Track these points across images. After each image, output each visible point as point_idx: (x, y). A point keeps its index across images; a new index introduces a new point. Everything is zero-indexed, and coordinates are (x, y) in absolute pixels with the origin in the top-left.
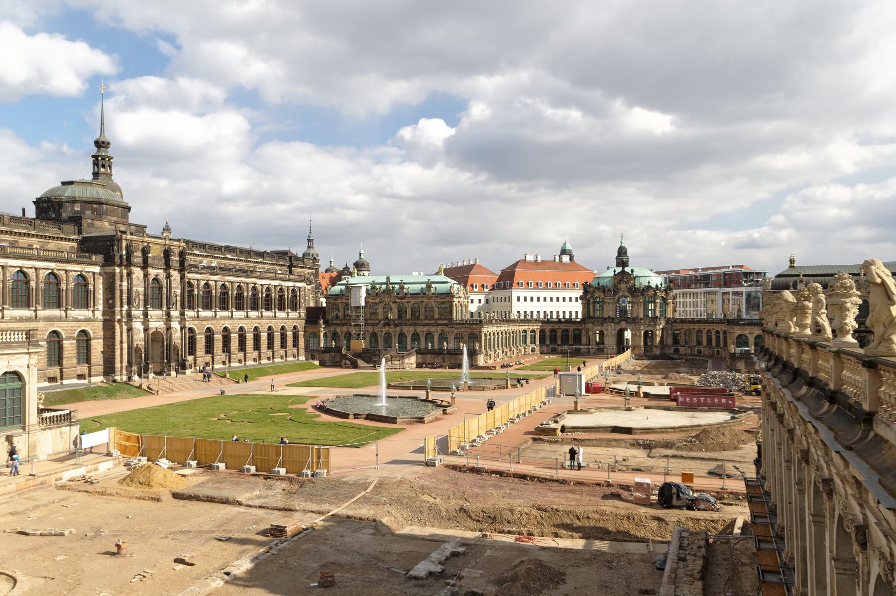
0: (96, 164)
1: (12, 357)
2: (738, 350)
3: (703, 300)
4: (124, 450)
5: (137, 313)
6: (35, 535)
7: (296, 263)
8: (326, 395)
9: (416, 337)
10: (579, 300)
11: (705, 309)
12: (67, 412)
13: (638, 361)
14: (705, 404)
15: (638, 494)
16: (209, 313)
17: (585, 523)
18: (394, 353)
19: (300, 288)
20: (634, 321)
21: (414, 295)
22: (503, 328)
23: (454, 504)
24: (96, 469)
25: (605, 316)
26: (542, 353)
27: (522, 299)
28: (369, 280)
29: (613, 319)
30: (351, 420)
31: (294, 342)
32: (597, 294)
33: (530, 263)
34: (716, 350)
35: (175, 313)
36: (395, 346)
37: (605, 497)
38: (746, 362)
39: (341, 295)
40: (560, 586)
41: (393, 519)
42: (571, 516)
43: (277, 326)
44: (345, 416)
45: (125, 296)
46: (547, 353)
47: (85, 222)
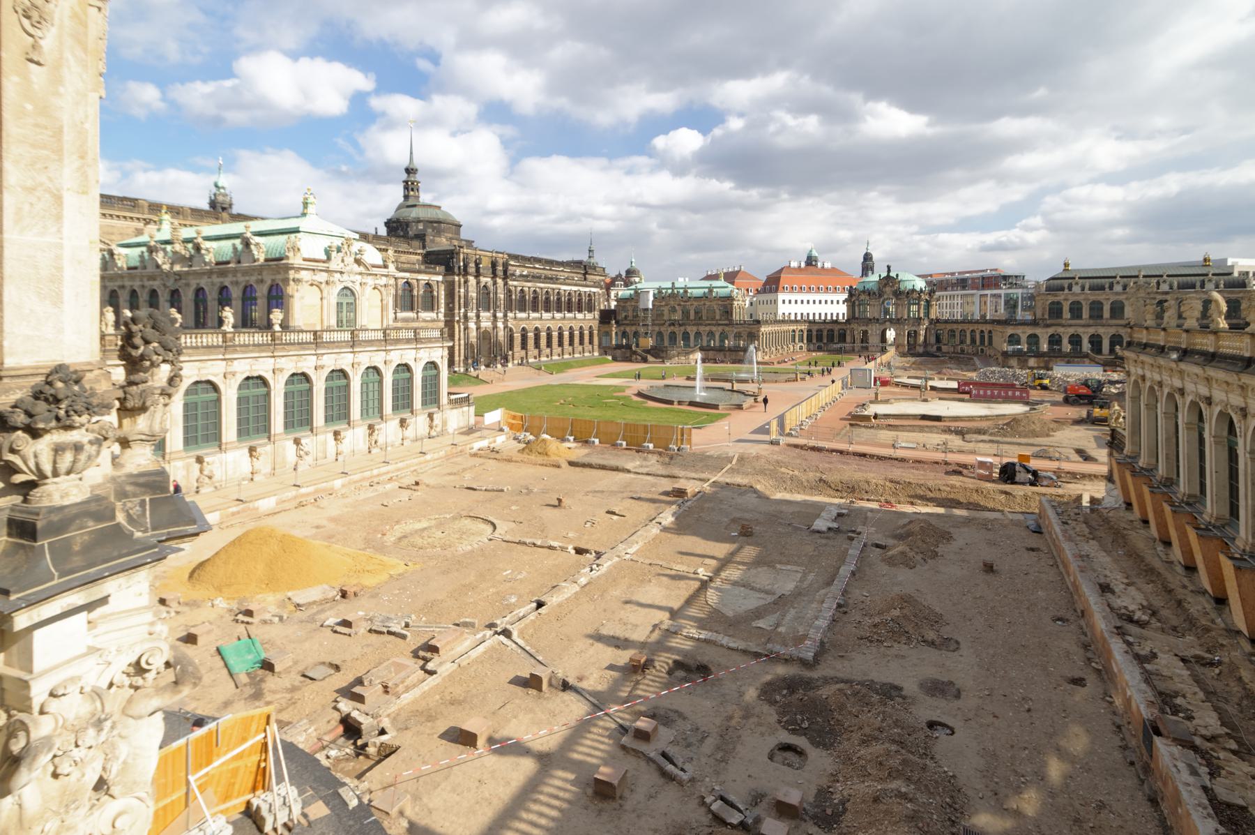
1: (432, 350)
2: (1011, 348)
4: (511, 427)
5: (472, 314)
8: (643, 385)
9: (698, 334)
12: (466, 395)
14: (992, 396)
15: (981, 471)
16: (536, 315)
20: (897, 322)
22: (776, 328)
23: (812, 475)
24: (495, 442)
26: (809, 350)
27: (787, 302)
28: (657, 285)
30: (676, 406)
32: (862, 297)
33: (794, 269)
35: (500, 315)
37: (947, 473)
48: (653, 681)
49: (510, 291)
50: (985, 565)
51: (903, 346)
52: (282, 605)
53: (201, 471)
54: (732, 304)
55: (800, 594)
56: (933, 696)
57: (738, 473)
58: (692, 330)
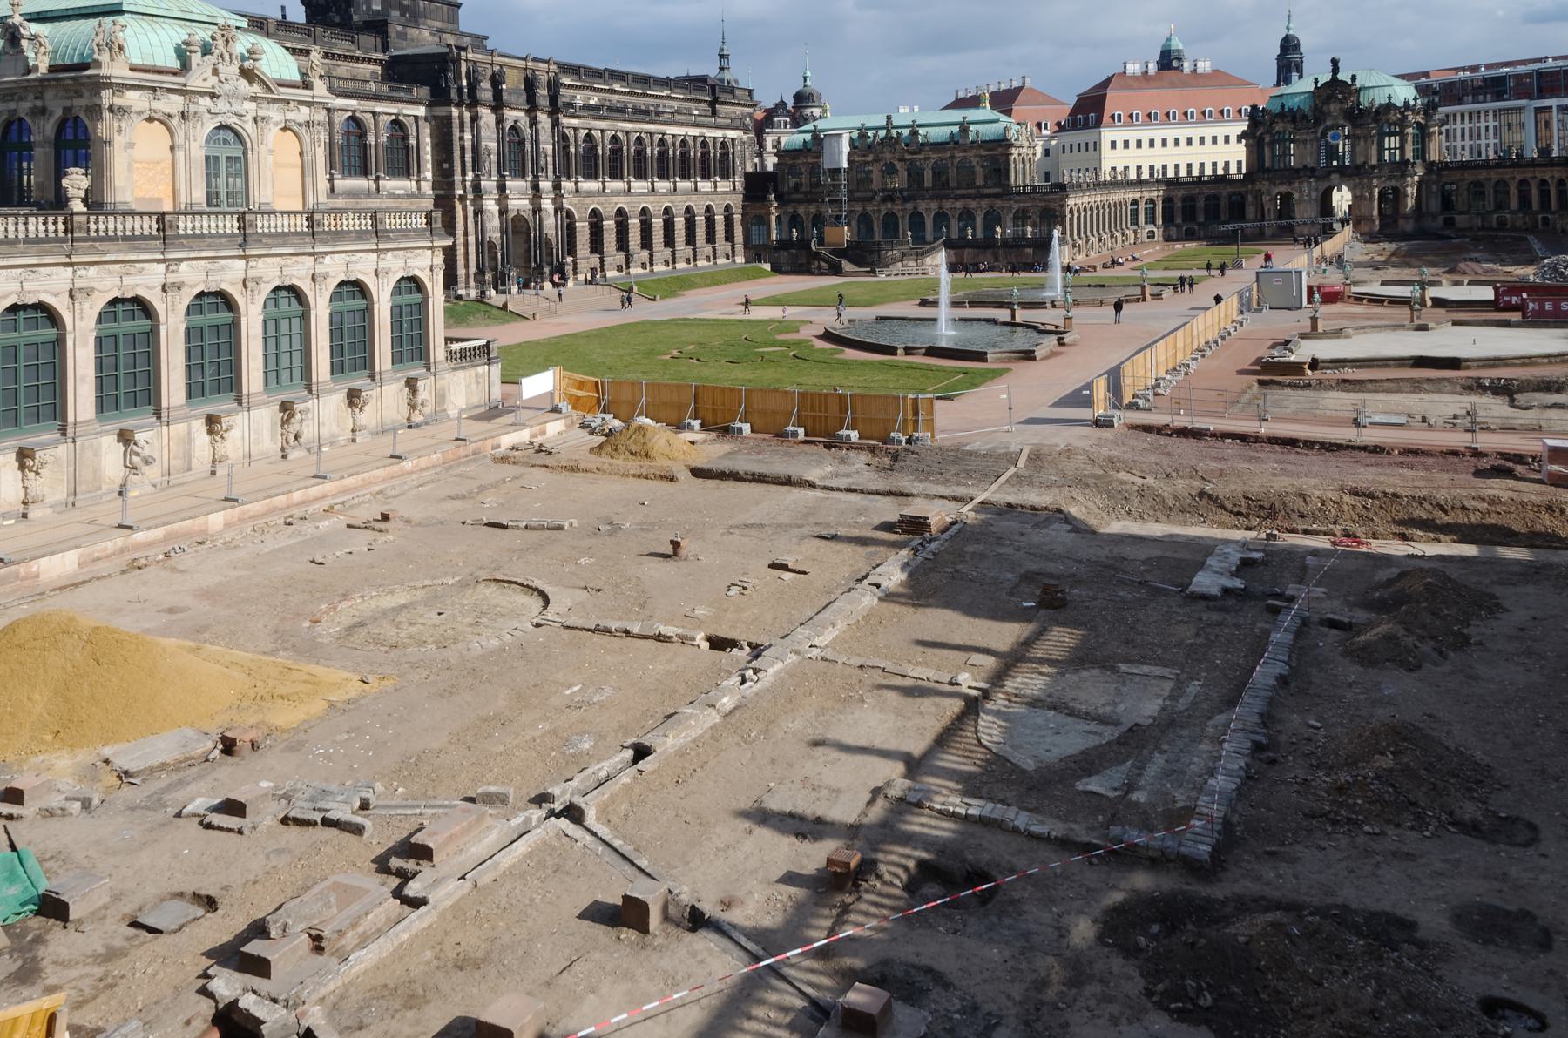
3: (1491, 124)
4: (576, 403)
5: (489, 184)
6: (517, 528)
9: (941, 217)
11: (1497, 141)
12: (483, 342)
13: (1368, 245)
15: (1557, 468)
16: (618, 185)
17: (1461, 519)
20: (1354, 173)
22: (1099, 198)
23: (1182, 485)
24: (543, 433)
26: (1167, 239)
30: (901, 357)
32: (1279, 127)
35: (546, 185)
36: (905, 235)
37: (1479, 473)
39: (805, 150)
41: (1083, 509)
42: (1426, 505)
45: (468, 156)
46: (1178, 240)
48: (876, 904)
49: (565, 138)
51: (1371, 220)
52: (89, 774)
54: (1008, 155)
55: (1172, 724)
56: (1486, 942)
57: (1031, 483)
58: (929, 208)
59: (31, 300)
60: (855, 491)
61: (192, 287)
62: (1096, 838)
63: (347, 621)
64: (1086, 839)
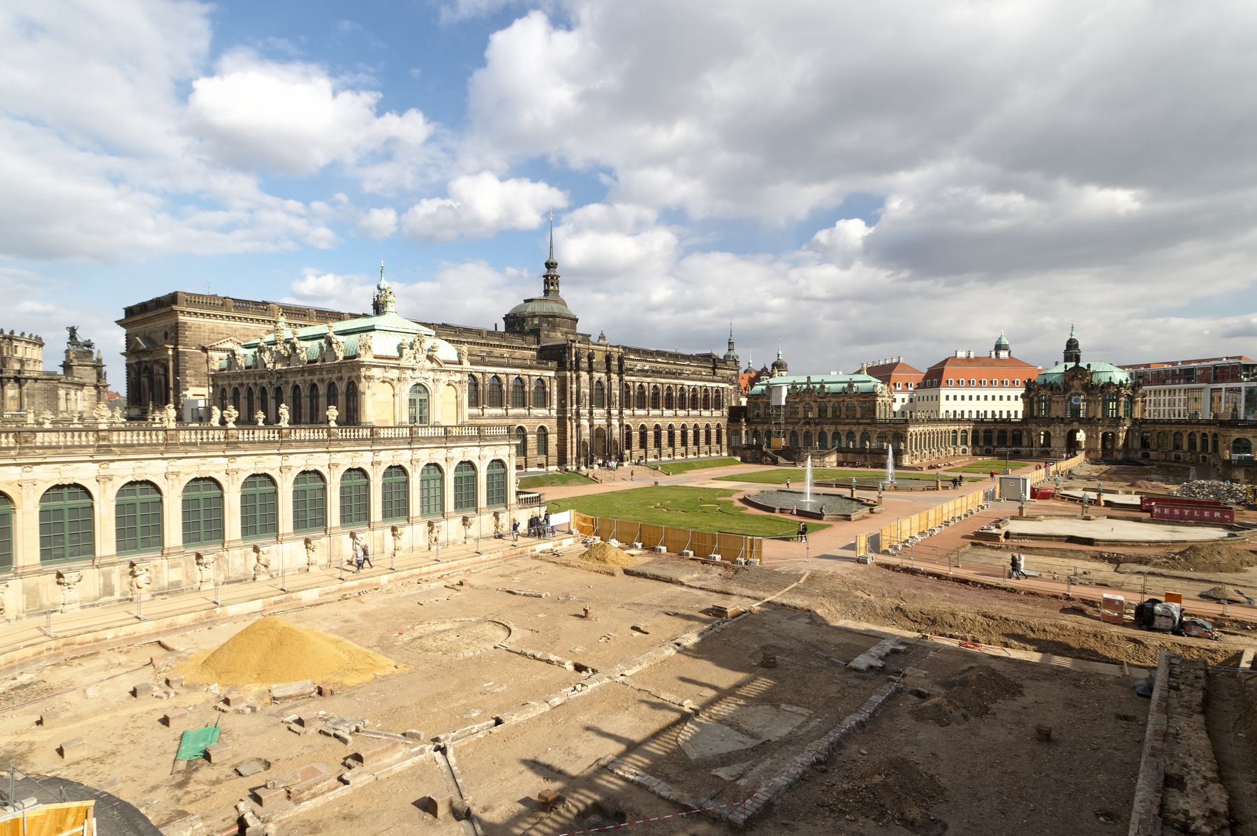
0: (546, 282)
1: (497, 448)
2: (1236, 456)
3: (1183, 397)
4: (582, 529)
5: (584, 411)
6: (520, 594)
7: (719, 365)
8: (752, 489)
9: (836, 435)
10: (1019, 398)
12: (538, 495)
13: (1093, 466)
14: (1191, 517)
16: (642, 412)
17: (1042, 636)
18: (814, 451)
19: (723, 388)
20: (1089, 422)
21: (835, 394)
23: (889, 602)
24: (561, 545)
25: (1054, 416)
26: (974, 454)
27: (951, 398)
28: (790, 379)
29: (1062, 419)
30: (777, 514)
31: (717, 439)
32: (1042, 392)
33: (961, 359)
34: (1201, 455)
35: (615, 412)
36: (815, 444)
37: (1064, 610)
38: (1247, 471)
39: (762, 395)
40: (1017, 698)
41: (827, 611)
42: (1023, 626)
43: (702, 424)
44: (772, 510)
46: (980, 455)
47: (543, 333)
50: (1039, 731)
51: (1096, 450)
53: (258, 560)
54: (875, 401)
57: (802, 593)
58: (829, 430)
59: (311, 469)
60: (703, 589)
61: (386, 463)
62: (692, 803)
63: (416, 634)
64: (686, 803)
